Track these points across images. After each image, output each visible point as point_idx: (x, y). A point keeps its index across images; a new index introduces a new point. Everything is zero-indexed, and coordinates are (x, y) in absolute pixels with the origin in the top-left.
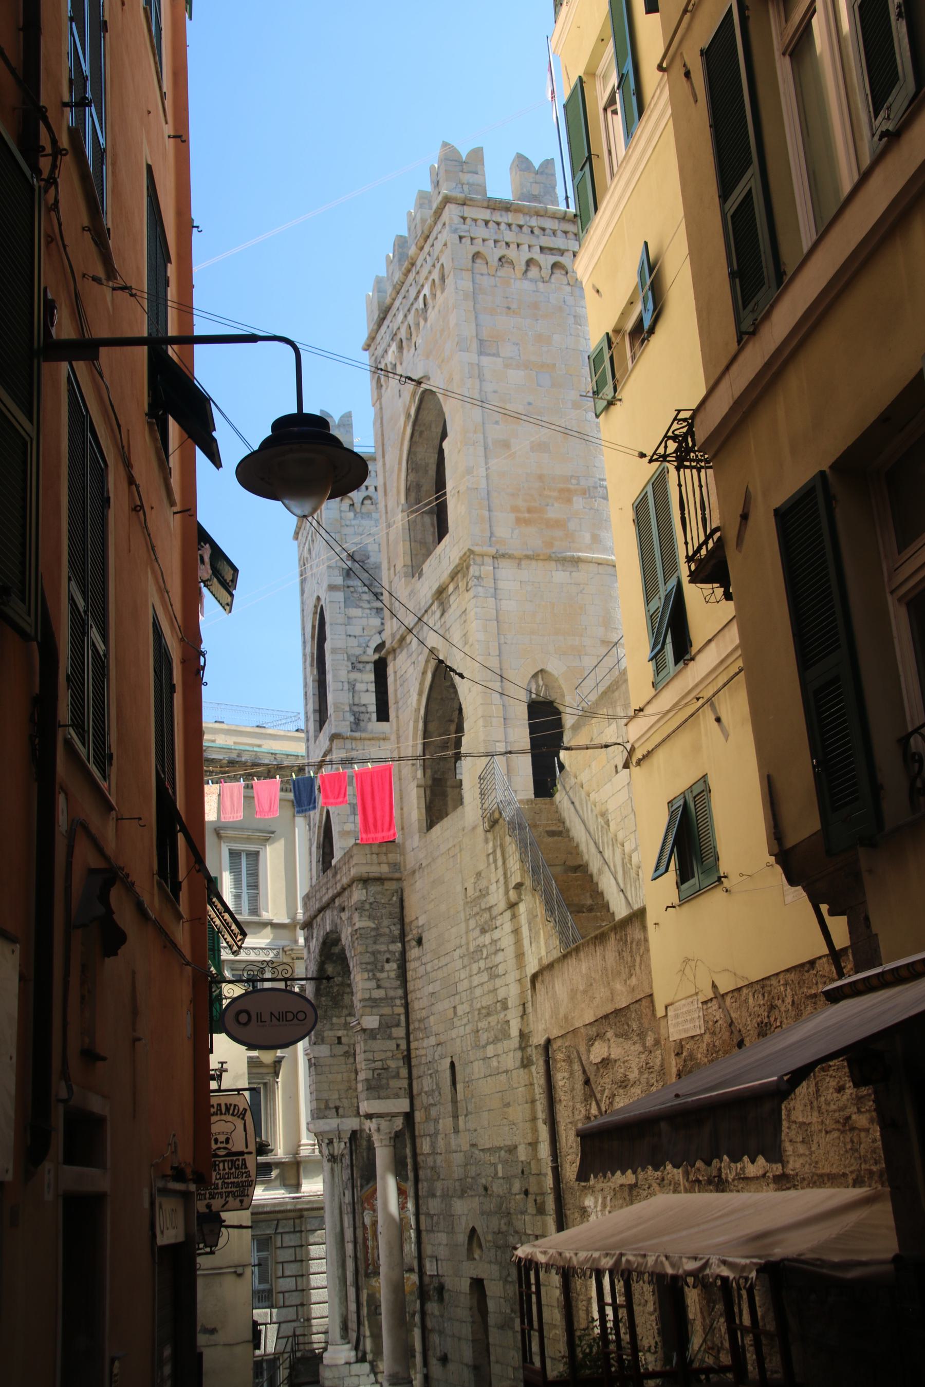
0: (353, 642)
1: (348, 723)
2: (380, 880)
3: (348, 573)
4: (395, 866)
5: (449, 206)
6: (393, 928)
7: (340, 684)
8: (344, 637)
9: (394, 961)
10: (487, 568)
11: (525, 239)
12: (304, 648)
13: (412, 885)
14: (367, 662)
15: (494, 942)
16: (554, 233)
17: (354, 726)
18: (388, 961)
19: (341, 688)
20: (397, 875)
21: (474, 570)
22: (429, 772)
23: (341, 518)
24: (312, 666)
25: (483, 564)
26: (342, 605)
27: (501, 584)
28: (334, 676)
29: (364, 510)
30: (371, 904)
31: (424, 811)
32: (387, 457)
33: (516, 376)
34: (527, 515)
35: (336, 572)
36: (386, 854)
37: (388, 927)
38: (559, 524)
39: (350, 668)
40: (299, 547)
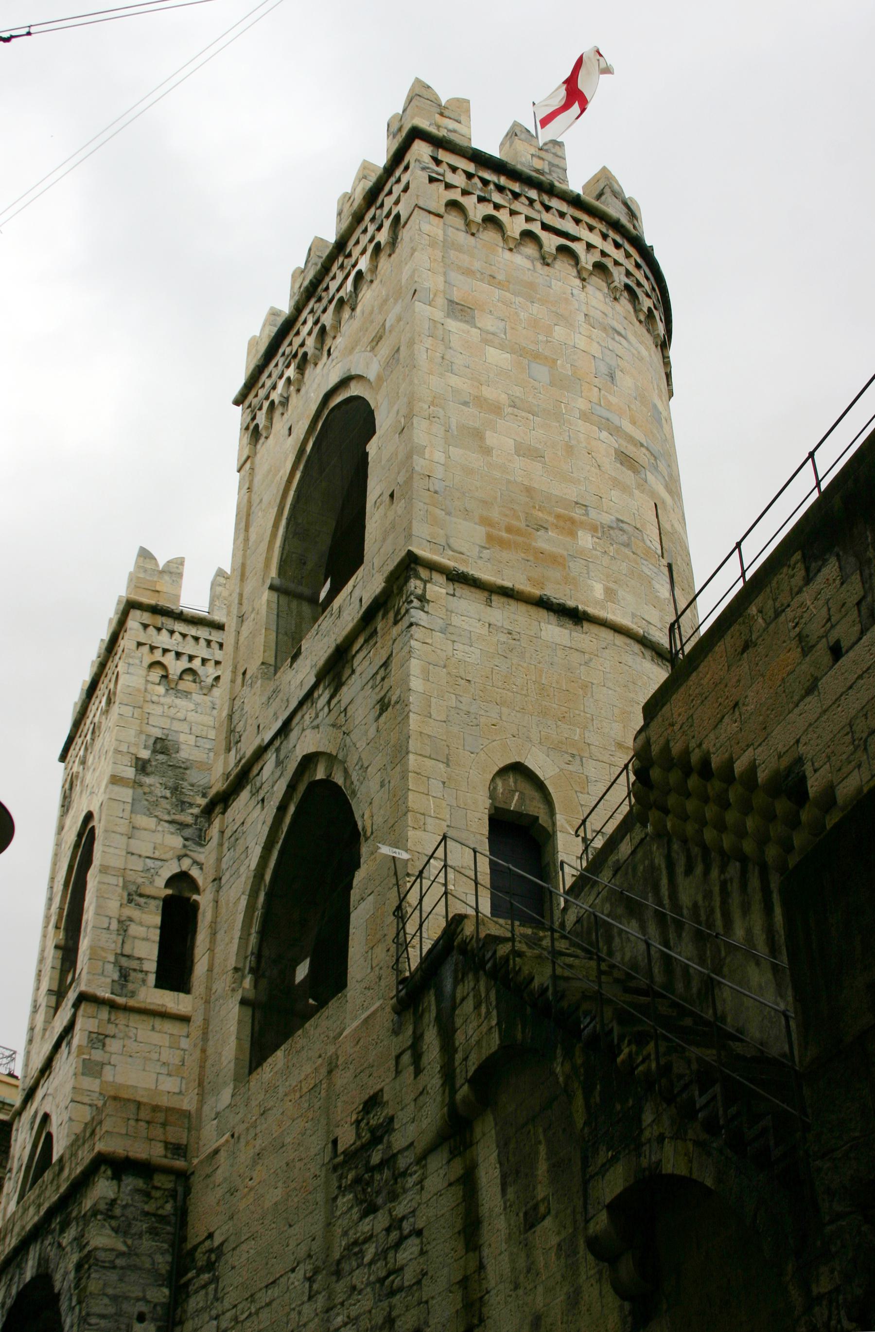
0: (137, 864)
1: (109, 980)
3: (142, 766)
6: (159, 1258)
7: (107, 920)
8: (124, 853)
9: (154, 1320)
12: (49, 907)
13: (208, 1176)
14: (154, 898)
15: (396, 1224)
16: (562, 215)
18: (141, 1318)
19: (106, 926)
20: (180, 1164)
22: (264, 982)
23: (146, 690)
24: (57, 927)
26: (128, 807)
27: (456, 620)
28: (99, 906)
29: (182, 686)
30: (125, 1207)
31: (247, 1045)
32: (252, 530)
33: (496, 356)
34: (504, 535)
35: (127, 760)
36: (164, 1125)
37: (150, 1256)
38: (555, 560)
39: (125, 901)
40: (66, 769)
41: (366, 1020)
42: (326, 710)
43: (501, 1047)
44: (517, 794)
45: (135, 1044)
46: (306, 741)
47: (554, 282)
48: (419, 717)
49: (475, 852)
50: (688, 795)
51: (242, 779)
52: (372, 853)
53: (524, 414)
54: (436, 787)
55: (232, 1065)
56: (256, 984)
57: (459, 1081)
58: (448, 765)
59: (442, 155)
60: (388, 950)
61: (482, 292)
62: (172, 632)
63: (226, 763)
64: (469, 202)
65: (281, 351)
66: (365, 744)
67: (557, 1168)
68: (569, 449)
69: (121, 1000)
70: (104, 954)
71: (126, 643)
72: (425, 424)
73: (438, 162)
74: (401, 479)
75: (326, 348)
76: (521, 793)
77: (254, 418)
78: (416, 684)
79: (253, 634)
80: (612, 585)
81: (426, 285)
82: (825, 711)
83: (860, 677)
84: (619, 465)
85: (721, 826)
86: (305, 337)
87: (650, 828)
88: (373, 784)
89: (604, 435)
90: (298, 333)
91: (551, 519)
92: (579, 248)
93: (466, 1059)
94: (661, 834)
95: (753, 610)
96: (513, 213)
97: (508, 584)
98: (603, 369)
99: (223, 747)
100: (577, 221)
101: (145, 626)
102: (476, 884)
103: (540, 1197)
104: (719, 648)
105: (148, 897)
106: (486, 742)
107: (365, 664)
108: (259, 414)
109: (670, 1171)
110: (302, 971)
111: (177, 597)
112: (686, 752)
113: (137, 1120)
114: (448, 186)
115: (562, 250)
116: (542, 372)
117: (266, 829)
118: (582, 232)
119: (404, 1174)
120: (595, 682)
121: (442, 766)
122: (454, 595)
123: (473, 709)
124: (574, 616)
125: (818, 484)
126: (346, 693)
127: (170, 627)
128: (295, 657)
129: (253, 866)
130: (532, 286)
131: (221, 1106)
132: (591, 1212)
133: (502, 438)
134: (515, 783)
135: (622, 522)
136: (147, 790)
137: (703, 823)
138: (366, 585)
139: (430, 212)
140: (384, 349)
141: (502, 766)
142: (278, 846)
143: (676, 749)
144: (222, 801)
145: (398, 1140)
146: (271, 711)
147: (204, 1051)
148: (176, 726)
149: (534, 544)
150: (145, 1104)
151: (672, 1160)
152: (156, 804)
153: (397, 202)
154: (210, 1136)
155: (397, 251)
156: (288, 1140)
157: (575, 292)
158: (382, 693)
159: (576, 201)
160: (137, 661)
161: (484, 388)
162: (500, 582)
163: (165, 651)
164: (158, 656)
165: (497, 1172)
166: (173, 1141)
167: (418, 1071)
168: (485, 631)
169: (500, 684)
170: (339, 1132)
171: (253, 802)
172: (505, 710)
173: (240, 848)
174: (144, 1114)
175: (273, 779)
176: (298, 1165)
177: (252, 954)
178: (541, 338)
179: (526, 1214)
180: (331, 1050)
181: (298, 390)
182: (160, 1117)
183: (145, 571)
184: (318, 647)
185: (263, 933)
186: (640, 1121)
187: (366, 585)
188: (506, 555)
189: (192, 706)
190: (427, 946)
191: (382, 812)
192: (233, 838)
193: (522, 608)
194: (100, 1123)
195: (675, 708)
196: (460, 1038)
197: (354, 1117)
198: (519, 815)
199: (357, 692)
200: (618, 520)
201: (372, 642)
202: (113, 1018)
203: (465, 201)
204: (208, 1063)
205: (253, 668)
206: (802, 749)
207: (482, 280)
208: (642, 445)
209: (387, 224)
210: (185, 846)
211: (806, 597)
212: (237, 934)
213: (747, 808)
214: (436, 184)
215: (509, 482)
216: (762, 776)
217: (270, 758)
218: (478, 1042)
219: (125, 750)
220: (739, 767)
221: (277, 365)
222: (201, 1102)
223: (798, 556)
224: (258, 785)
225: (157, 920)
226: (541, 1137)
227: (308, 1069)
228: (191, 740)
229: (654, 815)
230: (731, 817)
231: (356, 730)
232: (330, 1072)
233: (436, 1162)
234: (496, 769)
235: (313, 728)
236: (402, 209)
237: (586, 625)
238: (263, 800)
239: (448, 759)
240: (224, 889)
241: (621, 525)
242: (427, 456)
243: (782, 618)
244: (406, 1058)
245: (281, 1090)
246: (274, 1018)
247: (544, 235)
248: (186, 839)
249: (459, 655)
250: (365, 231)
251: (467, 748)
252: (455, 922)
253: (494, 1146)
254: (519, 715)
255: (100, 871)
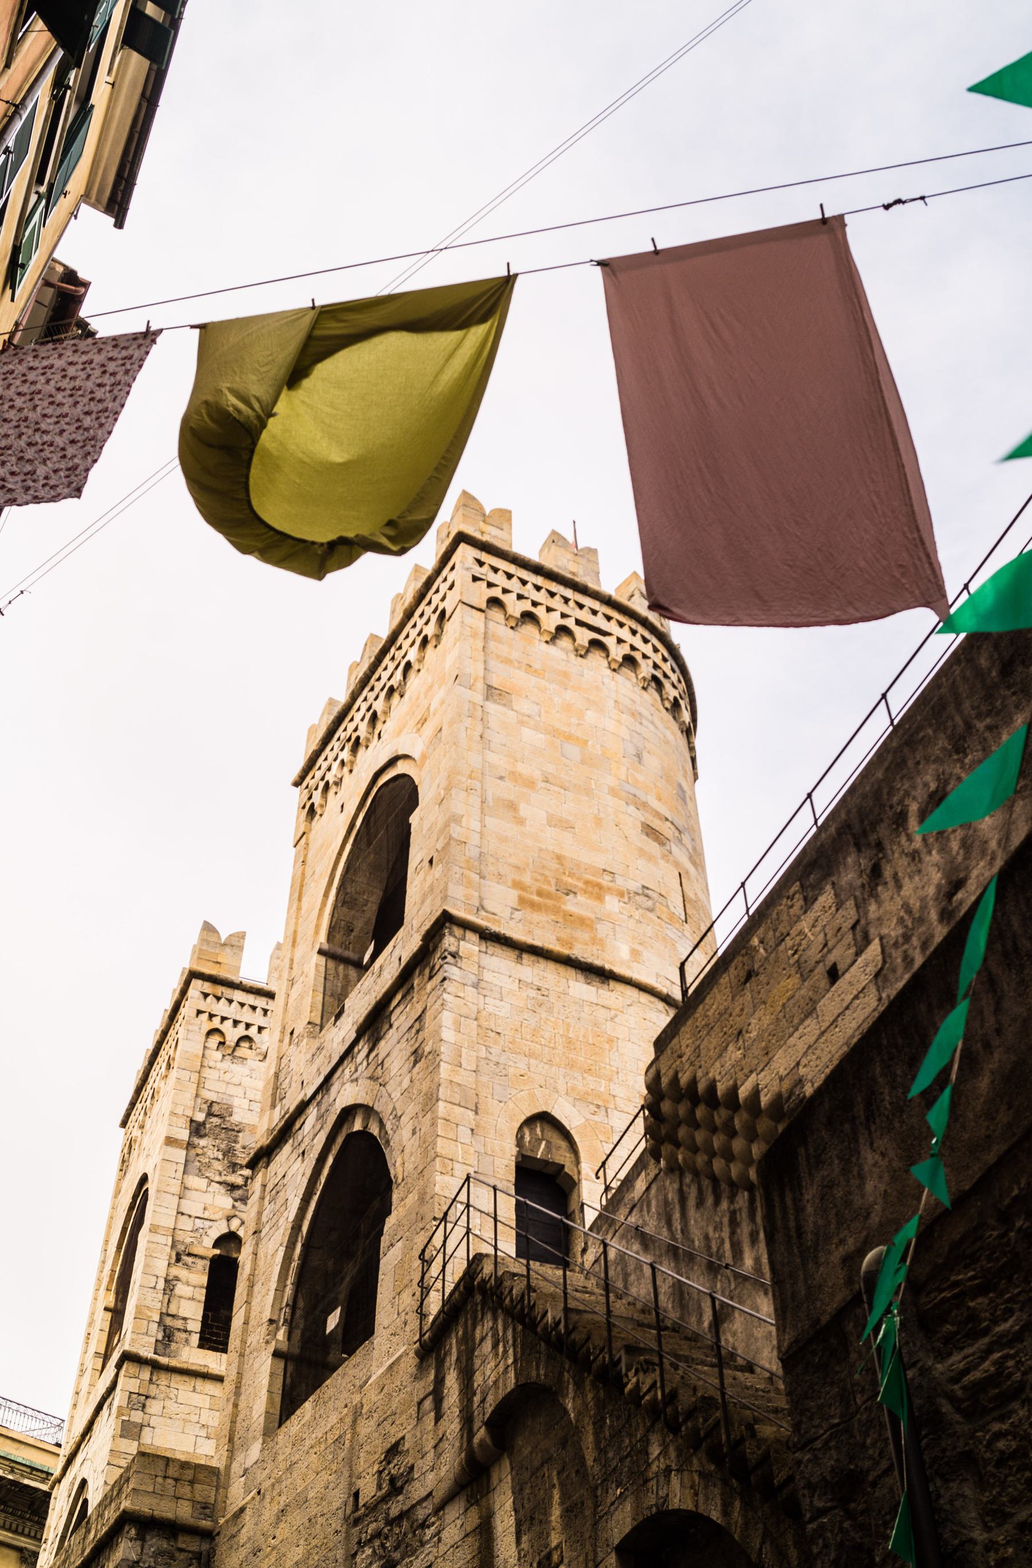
1: (153, 1340)
2: (171, 1529)
3: (197, 1129)
4: (207, 1509)
5: (463, 548)
10: (469, 946)
11: (556, 603)
14: (202, 1258)
16: (594, 612)
17: (160, 1346)
19: (152, 1285)
20: (206, 1524)
21: (449, 942)
22: (297, 1333)
25: (464, 939)
26: (181, 1168)
27: (487, 976)
31: (278, 1399)
32: (304, 899)
33: (531, 737)
35: (184, 1123)
36: (192, 1482)
38: (582, 922)
39: (173, 1261)
41: (391, 1367)
42: (365, 1063)
43: (518, 1386)
44: (544, 1143)
45: (176, 1405)
46: (346, 1093)
47: (586, 671)
48: (450, 1067)
49: (495, 1189)
50: (697, 1126)
51: (284, 1133)
52: (402, 1200)
53: (556, 789)
54: (464, 1133)
55: (262, 1419)
56: (290, 1336)
57: (477, 1424)
58: (476, 1113)
59: (484, 557)
60: (414, 1295)
61: (519, 678)
62: (230, 1001)
63: (270, 1119)
64: (509, 600)
65: (336, 736)
66: (399, 1095)
67: (570, 1512)
68: (598, 821)
69: (163, 1360)
70: (149, 1314)
71: (187, 1010)
72: (463, 795)
73: (481, 564)
74: (439, 846)
75: (377, 732)
76: (548, 1142)
77: (310, 798)
78: (448, 1034)
79: (301, 996)
80: (639, 948)
81: (468, 671)
82: (823, 1033)
83: (856, 997)
84: (645, 837)
85: (729, 1156)
86: (358, 723)
87: (662, 1162)
88: (405, 1133)
89: (631, 809)
90: (352, 720)
91: (580, 885)
92: (610, 642)
93: (483, 1401)
94: (674, 1169)
95: (755, 941)
96: (549, 610)
97: (538, 943)
98: (632, 750)
99: (269, 1103)
100: (609, 618)
101: (206, 995)
102: (496, 1221)
103: (554, 1544)
104: (724, 980)
105: (196, 1256)
106: (516, 1091)
107: (401, 1018)
108: (315, 793)
109: (676, 1506)
110: (333, 1321)
111: (238, 969)
112: (694, 1082)
113: (165, 1477)
114: (490, 585)
115: (595, 644)
116: (573, 751)
117: (305, 1181)
118: (612, 627)
119: (424, 1525)
120: (620, 1037)
121: (471, 1114)
122: (486, 953)
123: (502, 1060)
124: (602, 975)
125: (816, 823)
126: (383, 1047)
127: (229, 997)
128: (338, 1016)
129: (292, 1218)
130: (565, 674)
131: (249, 1463)
132: (601, 1555)
133: (535, 810)
134: (542, 1131)
135: (647, 888)
136: (200, 1151)
137: (712, 1154)
138: (405, 944)
139: (472, 607)
140: (429, 730)
141: (529, 1114)
142: (316, 1198)
143: (684, 1079)
144: (263, 1156)
145: (417, 1491)
146: (315, 1067)
147: (236, 1405)
148: (232, 1090)
149: (563, 907)
150: (174, 1460)
151: (678, 1495)
152: (209, 1166)
153: (443, 599)
154: (237, 1494)
155: (442, 642)
156: (311, 1494)
157: (606, 680)
158: (417, 1045)
159: (608, 601)
160: (197, 1028)
161: (519, 764)
162: (529, 940)
163: (224, 1019)
164: (216, 1023)
165: (512, 1521)
166: (200, 1499)
167: (438, 1417)
168: (515, 986)
169: (528, 1037)
170: (360, 1484)
171: (294, 1156)
172: (532, 1061)
173: (280, 1200)
174: (172, 1471)
175: (313, 1132)
176: (320, 1520)
177: (287, 1305)
178: (574, 721)
179: (539, 1563)
180: (356, 1399)
181: (351, 771)
182: (189, 1474)
183: (208, 942)
184: (359, 1003)
185: (298, 1285)
186: (647, 1454)
187: (405, 944)
188: (536, 917)
189: (248, 1072)
190: (449, 1287)
191: (413, 1159)
192: (274, 1192)
193: (551, 966)
194: (128, 1480)
195: (685, 1041)
196: (478, 1379)
197: (376, 1467)
198: (546, 1163)
199: (394, 1045)
200: (644, 887)
201: (409, 998)
202: (154, 1378)
203: (504, 598)
204: (241, 1416)
205: (300, 1027)
206: (802, 1071)
207: (519, 668)
208: (667, 819)
209: (434, 618)
210: (234, 1207)
211: (805, 925)
212: (273, 1285)
213: (752, 1136)
214: (479, 583)
215: (541, 850)
216: (765, 1100)
217: (312, 1113)
218: (495, 1382)
219: (181, 1113)
220: (743, 1092)
221: (332, 749)
222: (231, 1458)
223: (796, 886)
224: (300, 1138)
225: (204, 1280)
226: (555, 1481)
227: (334, 1419)
228: (245, 1103)
229: (666, 1149)
230: (738, 1145)
231: (391, 1082)
232: (355, 1422)
233: (453, 1512)
234: (523, 1118)
235: (352, 1081)
236: (448, 605)
237: (612, 983)
238: (303, 1153)
239: (477, 1107)
240: (264, 1241)
241: (647, 891)
242: (464, 824)
243: (782, 947)
244: (428, 1404)
245: (308, 1443)
246: (306, 1368)
247: (577, 630)
248: (236, 1200)
249: (490, 1009)
250: (414, 626)
251: (495, 1097)
252: (475, 1262)
253: (509, 1493)
254: (546, 1067)
255: (150, 1231)
